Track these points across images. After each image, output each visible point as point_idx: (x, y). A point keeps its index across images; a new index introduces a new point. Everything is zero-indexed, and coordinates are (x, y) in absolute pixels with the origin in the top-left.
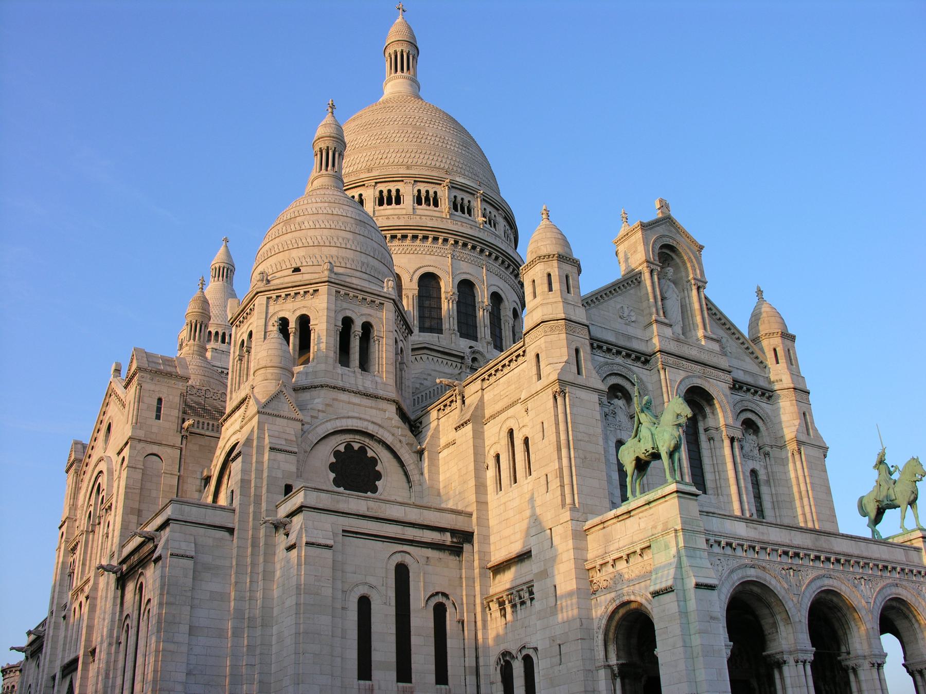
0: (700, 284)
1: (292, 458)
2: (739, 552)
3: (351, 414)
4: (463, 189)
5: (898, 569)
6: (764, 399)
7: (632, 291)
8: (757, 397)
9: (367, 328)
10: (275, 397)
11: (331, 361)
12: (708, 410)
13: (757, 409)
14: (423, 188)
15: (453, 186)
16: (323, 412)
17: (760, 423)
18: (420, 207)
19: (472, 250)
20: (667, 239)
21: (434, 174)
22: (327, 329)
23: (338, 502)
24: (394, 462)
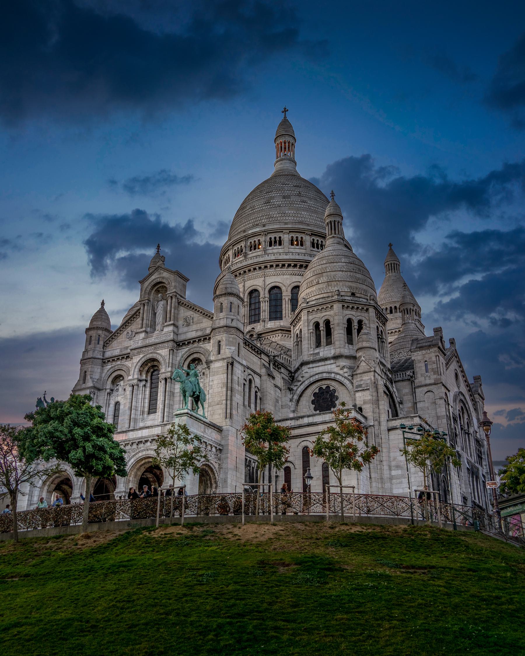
0: (171, 295)
4: (254, 235)
5: (150, 439)
8: (201, 344)
13: (201, 350)
21: (239, 237)
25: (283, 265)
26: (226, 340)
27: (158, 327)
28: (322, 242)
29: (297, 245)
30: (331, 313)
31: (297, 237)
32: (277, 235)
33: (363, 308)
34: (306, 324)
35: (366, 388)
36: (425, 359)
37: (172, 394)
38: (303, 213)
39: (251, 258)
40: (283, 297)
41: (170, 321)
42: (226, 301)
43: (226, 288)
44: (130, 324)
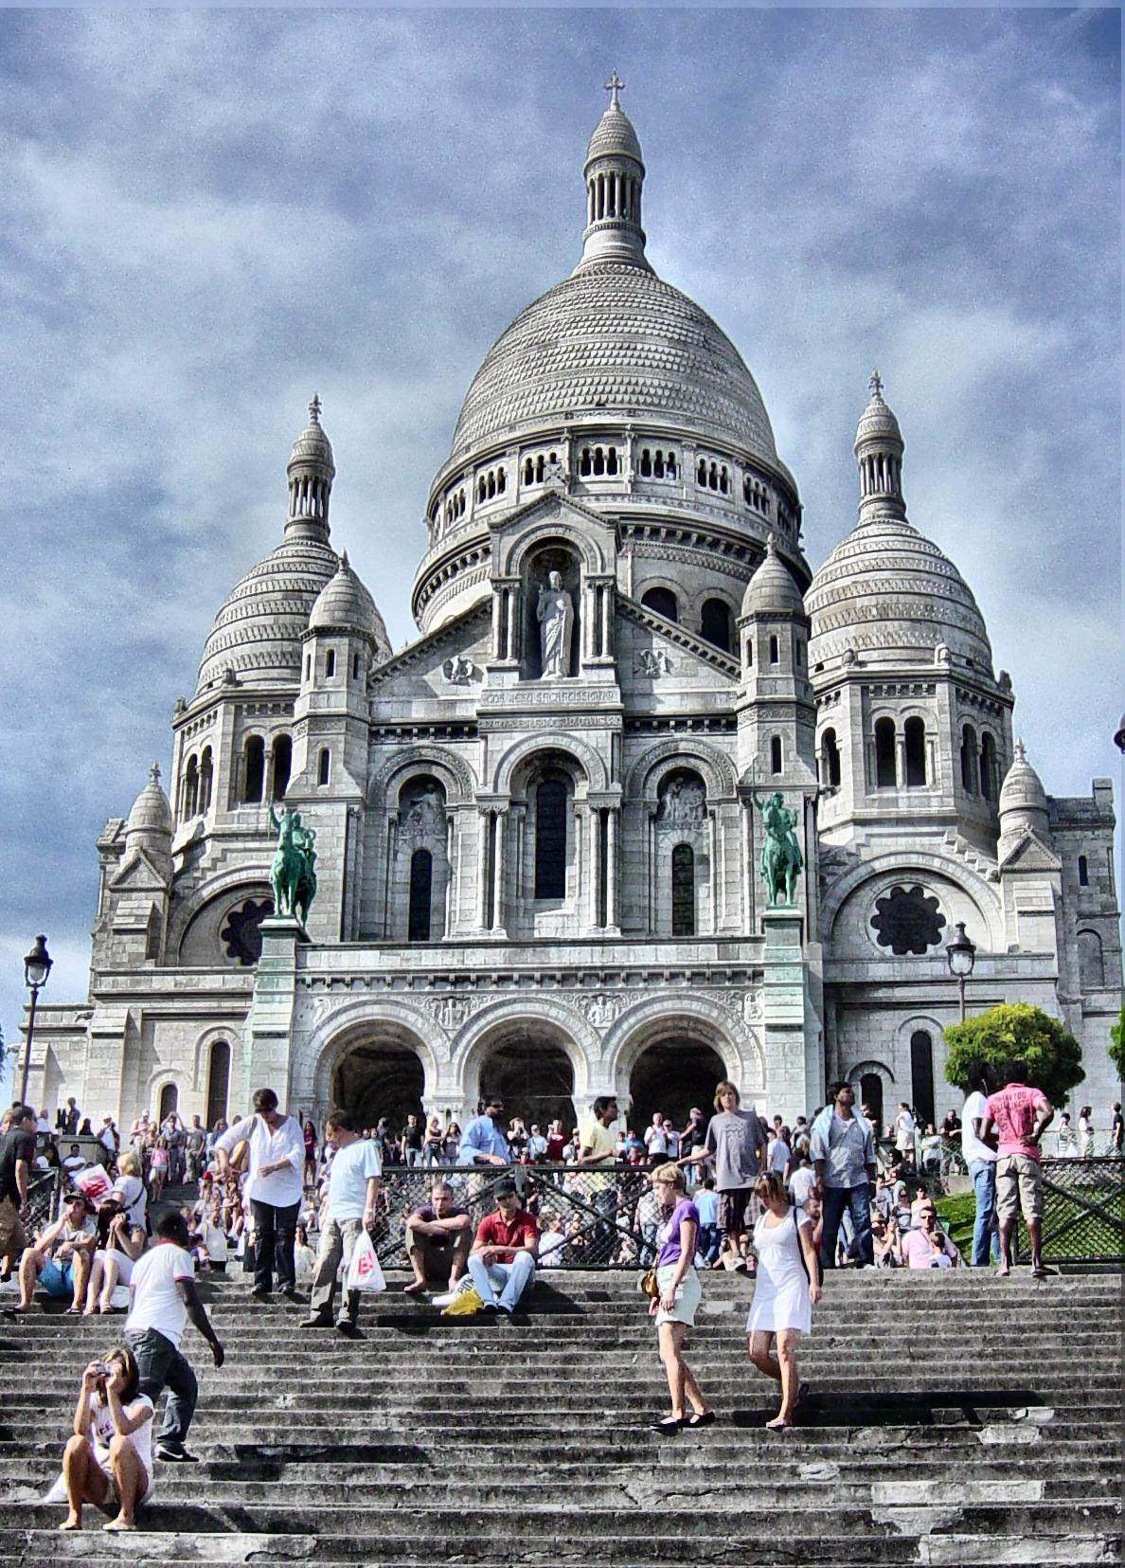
0: (598, 583)
1: (143, 938)
3: (246, 864)
4: (599, 432)
5: (688, 973)
10: (134, 867)
11: (225, 802)
12: (578, 775)
14: (533, 455)
15: (578, 435)
16: (209, 869)
17: (704, 771)
18: (529, 488)
20: (546, 531)
21: (548, 425)
23: (138, 983)
25: (687, 536)
26: (798, 738)
29: (714, 487)
30: (932, 703)
31: (714, 465)
33: (992, 705)
38: (721, 400)
39: (597, 497)
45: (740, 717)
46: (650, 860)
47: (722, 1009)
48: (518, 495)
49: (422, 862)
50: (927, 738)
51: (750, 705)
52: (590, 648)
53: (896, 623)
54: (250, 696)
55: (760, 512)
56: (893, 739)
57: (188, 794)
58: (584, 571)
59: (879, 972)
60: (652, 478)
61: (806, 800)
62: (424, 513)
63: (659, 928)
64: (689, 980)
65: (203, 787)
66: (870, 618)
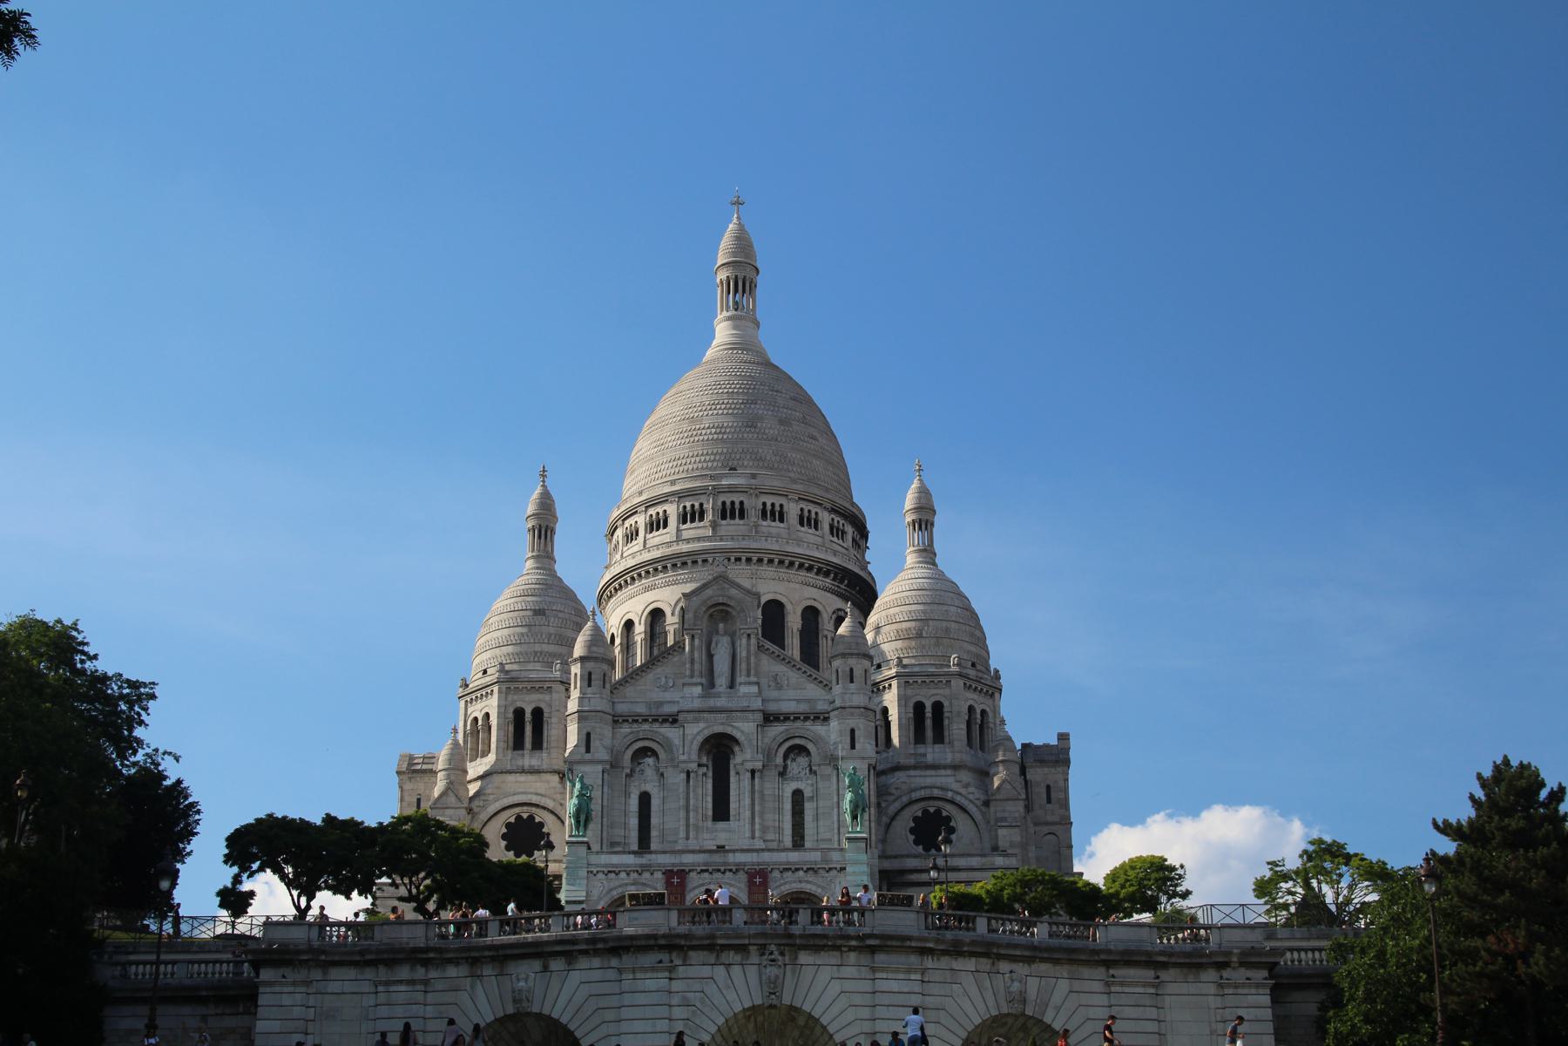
0: (749, 631)
2: (623, 875)
4: (732, 490)
5: (805, 868)
6: (818, 722)
7: (676, 659)
9: (538, 713)
11: (501, 750)
12: (736, 749)
15: (717, 491)
16: (493, 794)
17: (810, 746)
18: (685, 526)
19: (738, 563)
22: (498, 724)
24: (559, 822)
25: (792, 564)
27: (722, 681)
28: (843, 525)
29: (809, 524)
30: (947, 691)
31: (809, 511)
32: (778, 501)
33: (987, 691)
34: (903, 702)
35: (1014, 824)
36: (1048, 783)
37: (762, 795)
40: (790, 624)
41: (748, 675)
42: (859, 666)
43: (857, 644)
44: (660, 664)
45: (832, 714)
46: (779, 799)
47: (823, 888)
48: (678, 530)
49: (645, 799)
50: (946, 715)
51: (838, 709)
52: (744, 672)
53: (927, 640)
54: (513, 680)
55: (840, 542)
56: (924, 713)
57: (471, 743)
58: (738, 625)
59: (912, 863)
60: (768, 522)
61: (869, 765)
62: (606, 532)
63: (785, 839)
64: (805, 872)
65: (483, 740)
66: (911, 636)
